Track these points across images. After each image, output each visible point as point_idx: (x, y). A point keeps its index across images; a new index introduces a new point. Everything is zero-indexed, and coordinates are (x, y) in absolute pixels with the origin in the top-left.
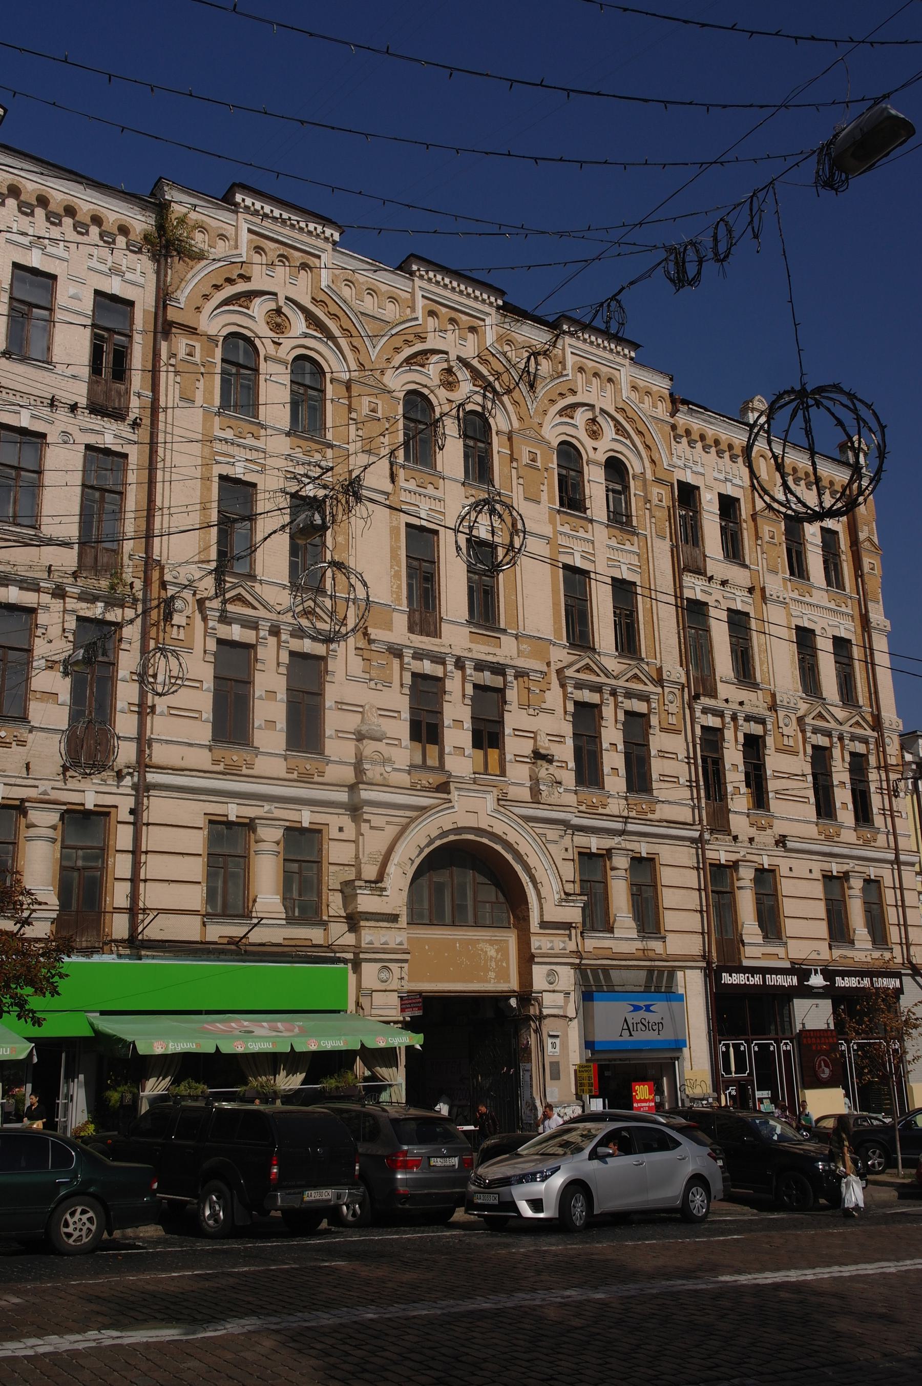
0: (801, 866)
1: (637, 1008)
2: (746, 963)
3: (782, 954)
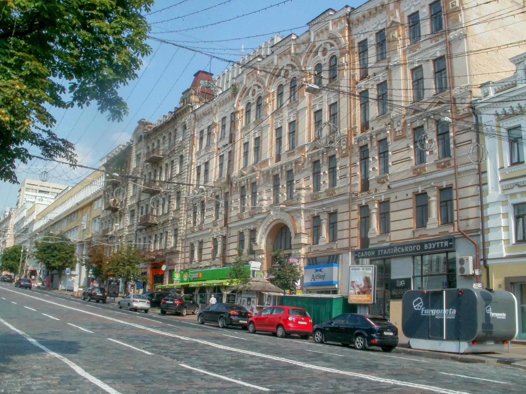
0: (401, 195)
1: (317, 271)
2: (370, 247)
3: (388, 240)
